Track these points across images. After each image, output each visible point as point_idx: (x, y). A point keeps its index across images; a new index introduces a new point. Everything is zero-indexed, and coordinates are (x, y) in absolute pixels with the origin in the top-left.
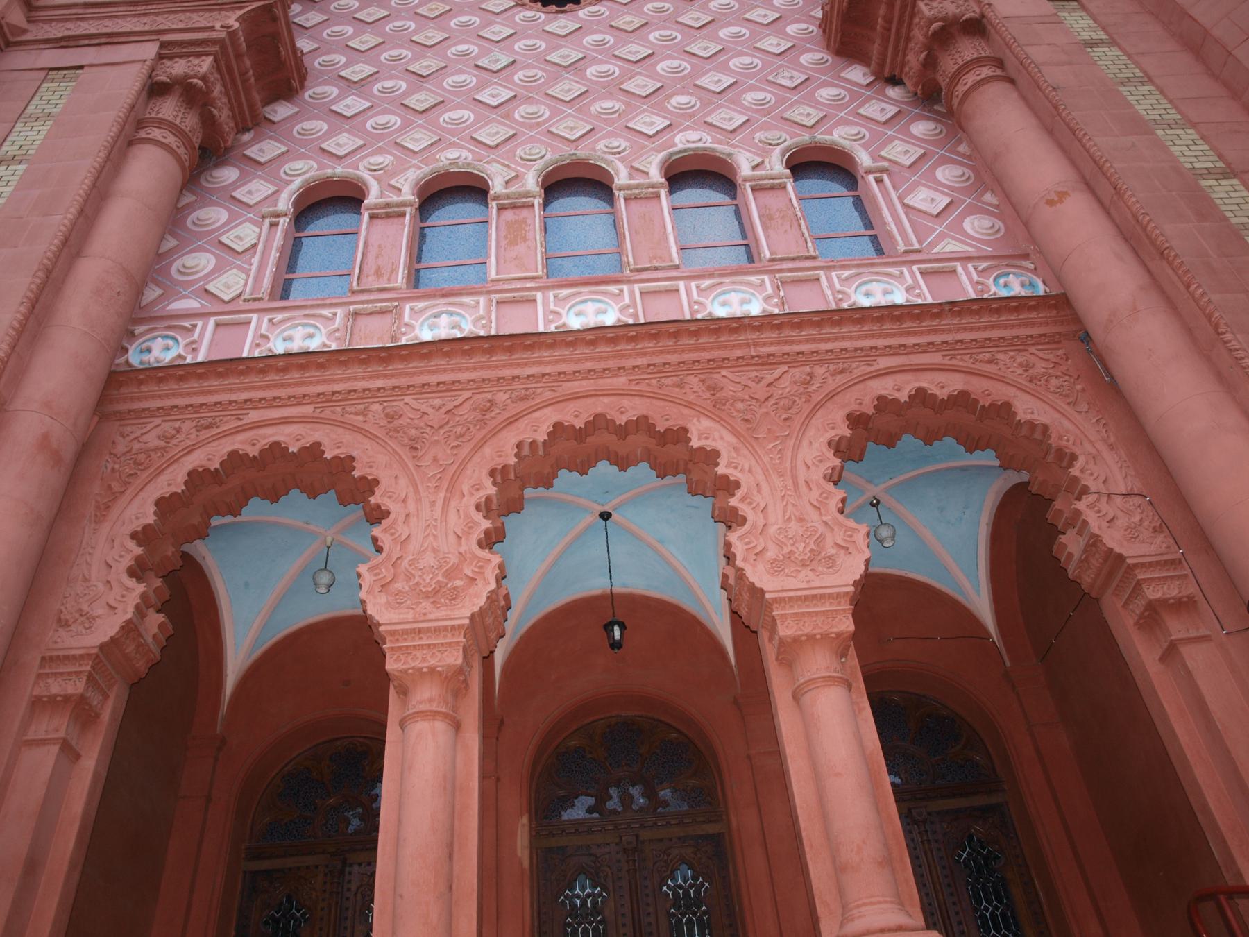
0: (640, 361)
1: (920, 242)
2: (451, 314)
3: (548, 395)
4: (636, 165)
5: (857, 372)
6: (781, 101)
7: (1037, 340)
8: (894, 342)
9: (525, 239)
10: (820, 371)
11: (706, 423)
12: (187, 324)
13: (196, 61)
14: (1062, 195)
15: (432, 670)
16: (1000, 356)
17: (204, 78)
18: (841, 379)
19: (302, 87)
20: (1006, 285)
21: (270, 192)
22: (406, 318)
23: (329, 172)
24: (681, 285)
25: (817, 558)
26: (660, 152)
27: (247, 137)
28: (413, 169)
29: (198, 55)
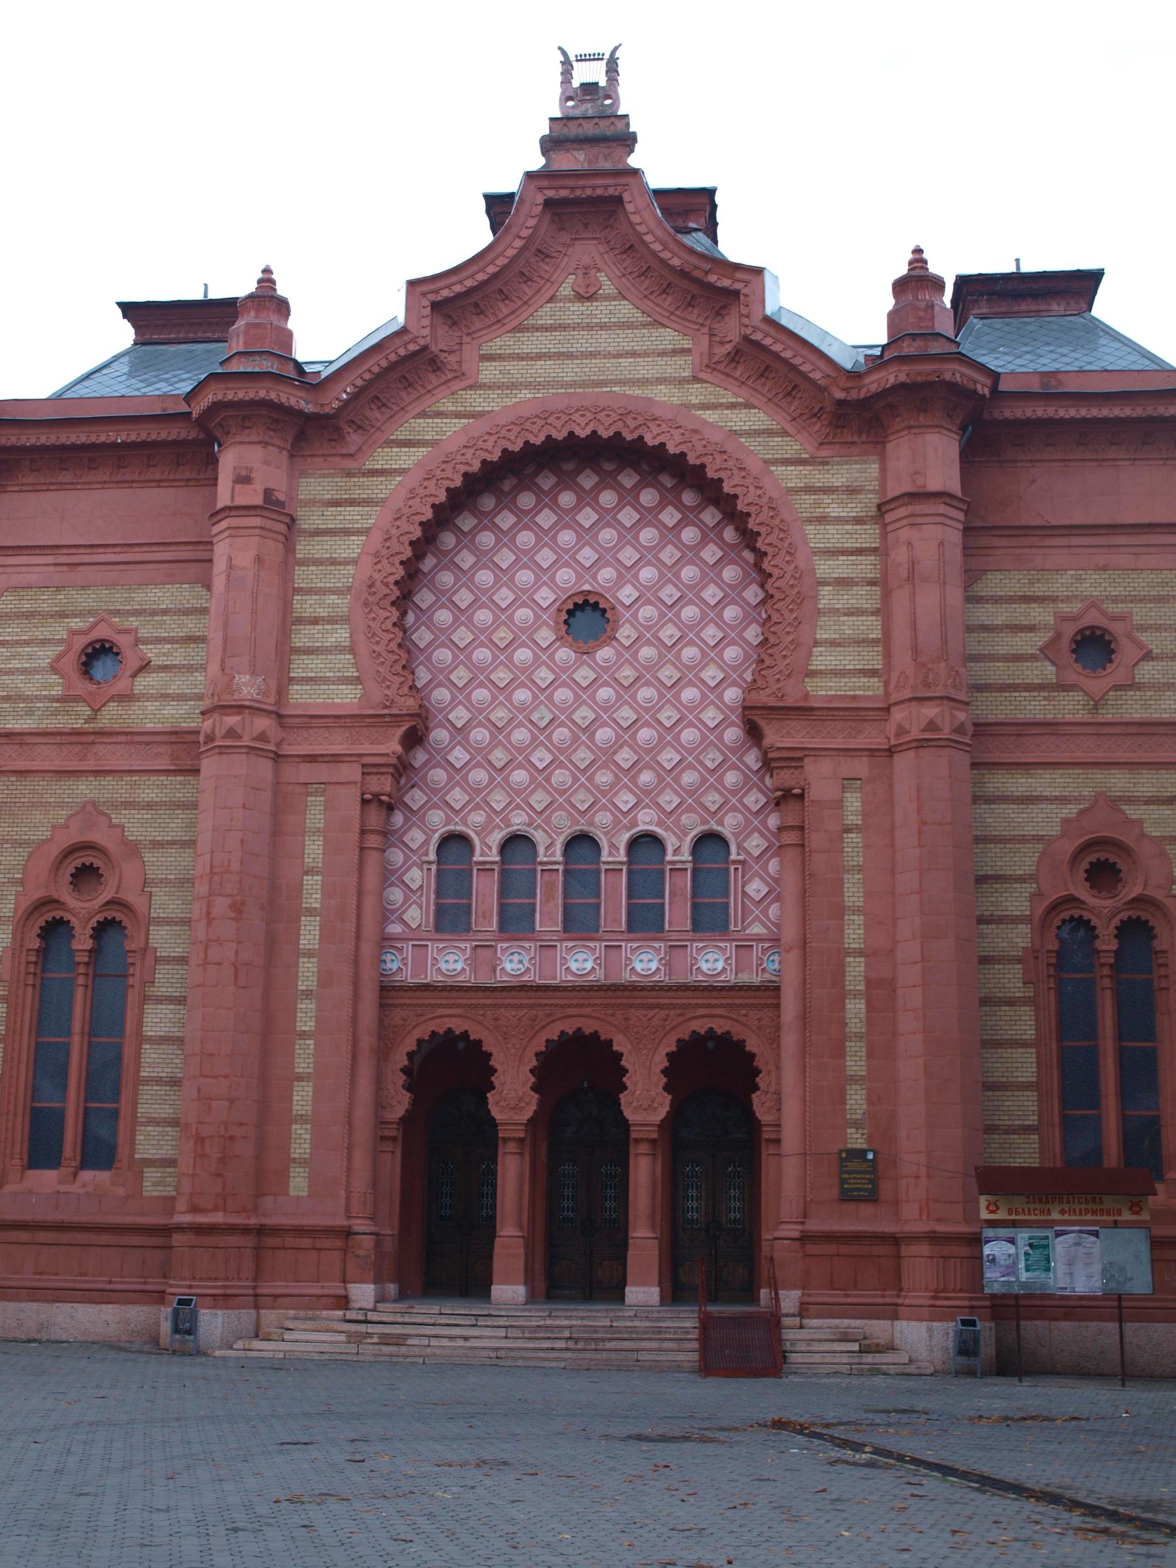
0: (598, 1001)
1: (742, 923)
2: (519, 954)
3: (559, 1015)
4: (614, 842)
5: (688, 1016)
6: (704, 780)
7: (768, 1006)
8: (706, 1001)
9: (554, 898)
10: (672, 1013)
11: (621, 1037)
12: (399, 945)
13: (383, 778)
14: (791, 948)
15: (514, 1139)
16: (751, 1013)
17: (389, 795)
18: (680, 1019)
19: (427, 728)
20: (773, 961)
21: (422, 840)
22: (499, 955)
23: (452, 827)
24: (623, 944)
25: (650, 1108)
26: (629, 829)
27: (403, 781)
28: (497, 831)
29: (382, 774)
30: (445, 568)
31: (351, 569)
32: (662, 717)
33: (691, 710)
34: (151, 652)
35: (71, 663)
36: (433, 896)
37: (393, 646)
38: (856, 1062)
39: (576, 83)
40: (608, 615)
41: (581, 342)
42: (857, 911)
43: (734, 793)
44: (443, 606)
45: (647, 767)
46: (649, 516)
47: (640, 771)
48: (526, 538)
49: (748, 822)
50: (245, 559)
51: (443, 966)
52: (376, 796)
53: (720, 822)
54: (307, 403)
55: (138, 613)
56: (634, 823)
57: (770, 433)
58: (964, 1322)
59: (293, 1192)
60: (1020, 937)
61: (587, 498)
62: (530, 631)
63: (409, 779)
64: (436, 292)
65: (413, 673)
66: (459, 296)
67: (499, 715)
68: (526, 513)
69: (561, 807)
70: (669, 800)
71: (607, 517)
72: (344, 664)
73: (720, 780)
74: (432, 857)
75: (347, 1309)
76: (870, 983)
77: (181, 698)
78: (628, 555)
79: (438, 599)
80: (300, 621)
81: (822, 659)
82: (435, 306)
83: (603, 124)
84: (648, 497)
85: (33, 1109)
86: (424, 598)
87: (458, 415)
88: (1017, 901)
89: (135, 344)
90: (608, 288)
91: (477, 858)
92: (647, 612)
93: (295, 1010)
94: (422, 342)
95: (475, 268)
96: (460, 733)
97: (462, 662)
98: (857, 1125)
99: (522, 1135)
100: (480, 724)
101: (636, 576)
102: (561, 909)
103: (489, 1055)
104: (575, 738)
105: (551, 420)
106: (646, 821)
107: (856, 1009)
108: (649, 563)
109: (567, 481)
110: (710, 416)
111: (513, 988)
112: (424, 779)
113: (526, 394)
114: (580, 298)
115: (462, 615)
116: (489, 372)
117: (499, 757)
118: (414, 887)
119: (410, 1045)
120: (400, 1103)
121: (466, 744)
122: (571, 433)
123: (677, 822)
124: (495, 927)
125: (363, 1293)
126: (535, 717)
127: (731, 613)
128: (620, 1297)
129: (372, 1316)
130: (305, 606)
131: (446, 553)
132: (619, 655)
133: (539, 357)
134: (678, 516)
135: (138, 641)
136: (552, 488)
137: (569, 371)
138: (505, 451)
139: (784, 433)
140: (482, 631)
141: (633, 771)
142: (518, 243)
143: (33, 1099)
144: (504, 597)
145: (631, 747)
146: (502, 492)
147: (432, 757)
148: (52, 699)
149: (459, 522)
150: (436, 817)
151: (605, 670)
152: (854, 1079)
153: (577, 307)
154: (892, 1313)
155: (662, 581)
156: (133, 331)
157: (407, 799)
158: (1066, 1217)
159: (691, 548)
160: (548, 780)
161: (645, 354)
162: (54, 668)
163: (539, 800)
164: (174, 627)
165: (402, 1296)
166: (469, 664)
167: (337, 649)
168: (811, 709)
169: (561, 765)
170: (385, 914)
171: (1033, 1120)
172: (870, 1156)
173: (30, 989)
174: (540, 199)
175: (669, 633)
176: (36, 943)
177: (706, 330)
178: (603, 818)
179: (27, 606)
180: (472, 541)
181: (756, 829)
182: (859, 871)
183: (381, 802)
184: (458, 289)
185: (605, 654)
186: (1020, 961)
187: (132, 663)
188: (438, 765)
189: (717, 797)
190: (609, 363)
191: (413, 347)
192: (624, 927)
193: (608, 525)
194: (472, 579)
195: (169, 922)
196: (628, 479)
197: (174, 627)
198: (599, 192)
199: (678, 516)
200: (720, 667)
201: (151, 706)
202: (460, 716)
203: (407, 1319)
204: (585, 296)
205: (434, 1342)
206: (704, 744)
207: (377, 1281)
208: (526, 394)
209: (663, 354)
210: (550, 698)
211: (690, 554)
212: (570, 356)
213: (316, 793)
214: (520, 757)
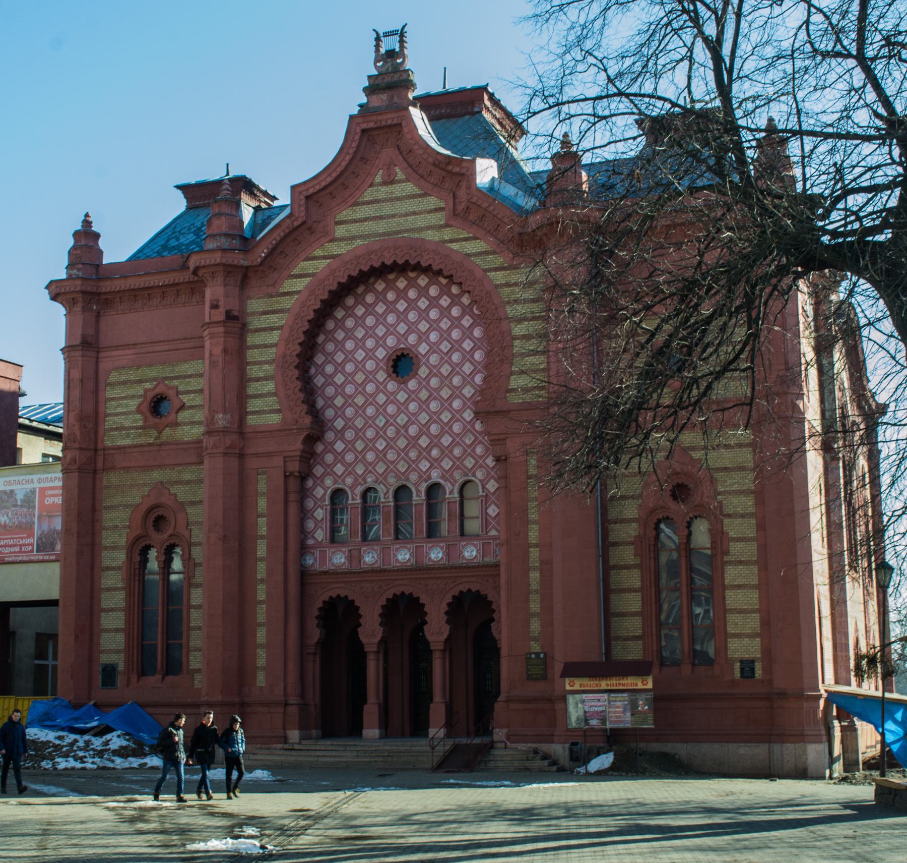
1: (486, 528)
6: (465, 451)
26: (426, 481)
27: (312, 461)
30: (330, 340)
31: (274, 350)
32: (443, 417)
33: (458, 411)
34: (185, 398)
35: (145, 408)
36: (328, 524)
37: (297, 390)
38: (535, 606)
39: (383, 51)
40: (414, 361)
41: (387, 209)
42: (536, 522)
43: (481, 457)
44: (330, 362)
45: (436, 445)
46: (434, 302)
47: (432, 448)
48: (370, 321)
49: (488, 473)
50: (218, 350)
51: (334, 561)
52: (292, 474)
53: (474, 475)
54: (244, 260)
55: (177, 378)
56: (429, 478)
57: (486, 253)
58: (573, 744)
59: (258, 684)
60: (631, 531)
61: (402, 294)
62: (374, 373)
63: (315, 461)
64: (307, 190)
65: (314, 402)
66: (320, 191)
67: (359, 423)
68: (370, 305)
69: (392, 471)
70: (447, 464)
71: (412, 305)
72: (272, 402)
73: (474, 450)
74: (327, 502)
75: (286, 742)
76: (542, 562)
77: (199, 423)
78: (423, 326)
79: (327, 359)
80: (251, 380)
81: (516, 382)
82: (307, 198)
83: (398, 75)
84: (433, 291)
85: (143, 645)
86: (319, 359)
87: (325, 258)
88: (631, 510)
89: (189, 208)
90: (400, 175)
91: (350, 502)
92: (434, 359)
93: (256, 589)
94: (300, 220)
95: (326, 175)
96: (340, 434)
97: (340, 393)
98: (535, 639)
99: (375, 649)
100: (350, 427)
101: (428, 337)
102: (392, 527)
103: (358, 608)
104: (398, 432)
105: (373, 256)
106: (435, 476)
107: (535, 576)
108: (435, 329)
109: (391, 286)
110: (455, 246)
111: (368, 572)
112: (323, 459)
113: (359, 242)
114: (385, 183)
115: (339, 368)
116: (340, 231)
117: (359, 445)
118: (319, 518)
119: (319, 604)
120: (315, 633)
121: (343, 439)
122: (383, 263)
123: (452, 475)
124: (360, 539)
125: (294, 735)
126: (377, 422)
127: (478, 356)
128: (426, 735)
129: (296, 747)
130: (253, 371)
131: (330, 332)
132: (420, 383)
133: (366, 220)
134: (449, 301)
135: (178, 393)
136: (384, 289)
137: (381, 227)
138: (349, 276)
139: (494, 253)
140: (350, 374)
141: (428, 449)
142: (348, 158)
143: (143, 640)
144: (360, 355)
145: (427, 435)
146: (357, 294)
147: (326, 447)
148: (137, 428)
149: (335, 313)
150: (328, 482)
151: (413, 392)
152: (534, 615)
153: (384, 189)
154: (550, 739)
155: (442, 339)
156: (185, 201)
157: (314, 471)
158: (609, 688)
159: (456, 319)
160: (385, 456)
161: (420, 213)
162: (139, 410)
163: (381, 468)
164: (196, 384)
165: (327, 734)
166: (344, 395)
167: (269, 394)
168: (509, 411)
169: (392, 448)
170: (303, 533)
171: (639, 632)
172: (542, 656)
173: (137, 583)
174: (358, 130)
175: (445, 370)
176: (138, 558)
177: (451, 196)
178: (413, 477)
179: (123, 378)
180: (343, 324)
181: (492, 477)
182: (536, 501)
183: (296, 477)
184: (318, 187)
185: (412, 384)
186: (632, 544)
187: (177, 405)
188: (329, 451)
189: (472, 460)
190: (402, 220)
191: (296, 224)
192: (424, 535)
193: (413, 309)
194: (343, 346)
195: (200, 544)
196: (423, 281)
197: (196, 384)
198: (389, 122)
199: (449, 301)
200: (472, 386)
201: (186, 428)
202: (339, 424)
203: (312, 748)
204: (389, 181)
205: (321, 759)
206: (465, 431)
207: (303, 727)
208: (359, 242)
209: (430, 211)
210: (385, 410)
211: (456, 323)
212: (381, 218)
213: (262, 474)
214: (370, 445)
